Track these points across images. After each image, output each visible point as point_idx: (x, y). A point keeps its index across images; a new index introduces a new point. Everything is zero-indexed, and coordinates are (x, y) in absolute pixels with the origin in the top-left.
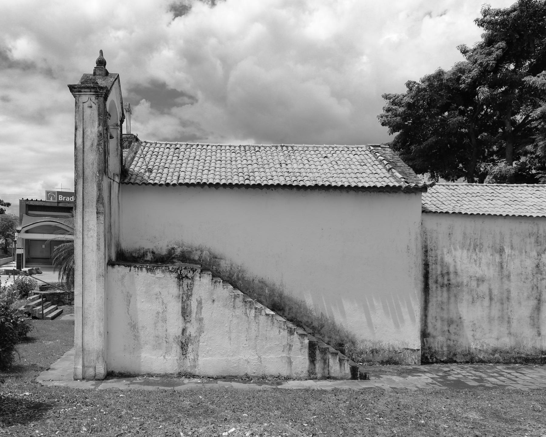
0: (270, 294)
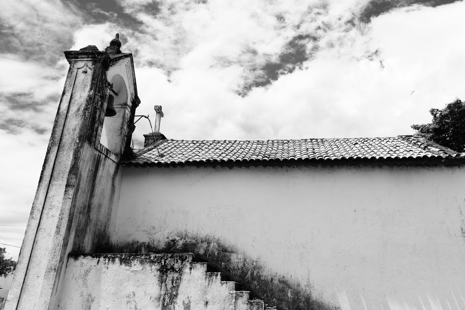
0: (293, 298)
